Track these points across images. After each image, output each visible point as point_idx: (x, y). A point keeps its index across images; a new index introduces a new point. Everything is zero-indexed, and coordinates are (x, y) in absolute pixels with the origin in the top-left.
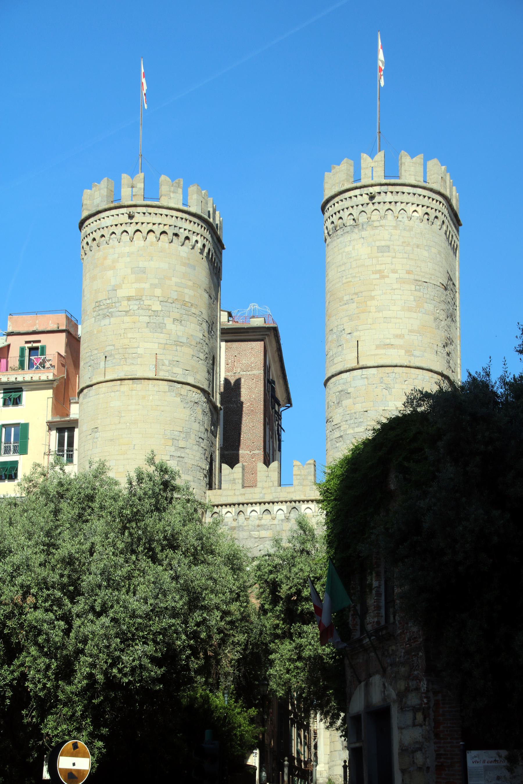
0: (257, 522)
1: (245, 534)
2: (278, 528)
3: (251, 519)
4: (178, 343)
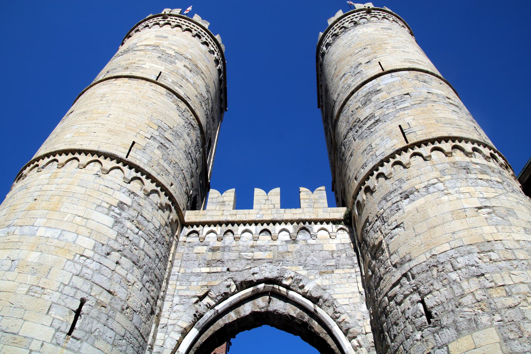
0: (251, 243)
1: (234, 255)
2: (281, 249)
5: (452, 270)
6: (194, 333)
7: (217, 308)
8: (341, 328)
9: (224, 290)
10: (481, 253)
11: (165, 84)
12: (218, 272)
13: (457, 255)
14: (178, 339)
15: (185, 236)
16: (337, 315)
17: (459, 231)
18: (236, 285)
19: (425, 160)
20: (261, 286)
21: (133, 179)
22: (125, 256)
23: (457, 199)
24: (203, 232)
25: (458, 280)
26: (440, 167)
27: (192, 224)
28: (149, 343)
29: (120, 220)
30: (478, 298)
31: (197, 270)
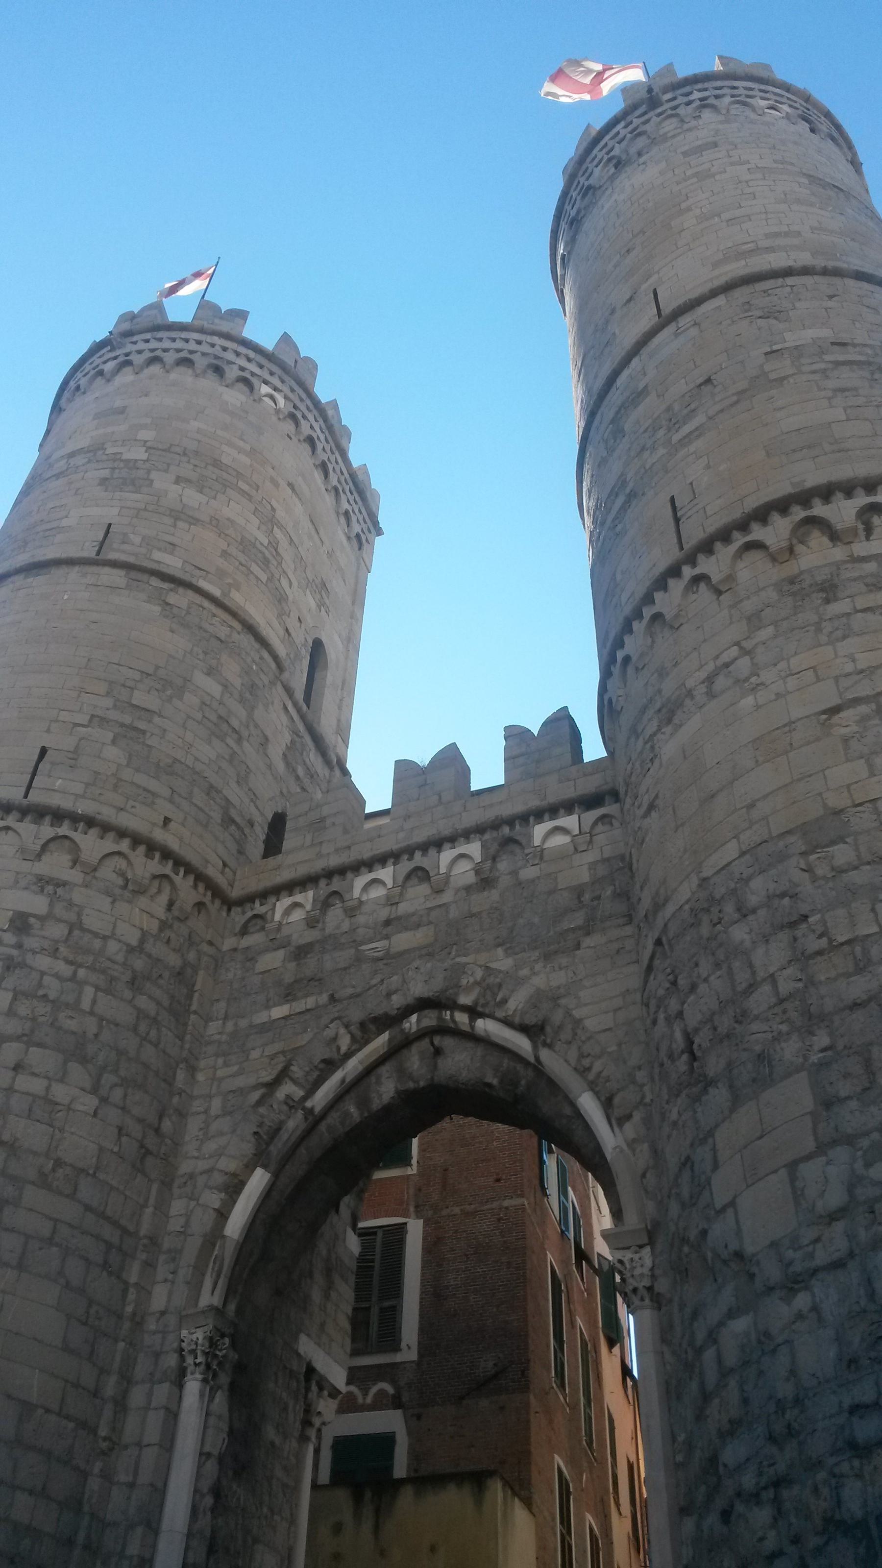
0: (384, 913)
1: (344, 957)
2: (454, 913)
3: (365, 908)
4: (180, 515)
5: (736, 916)
6: (259, 1180)
7: (308, 1104)
8: (597, 1094)
9: (320, 1053)
10: (813, 852)
11: (123, 557)
12: (308, 1010)
13: (751, 870)
14: (216, 1207)
15: (236, 935)
16: (586, 1062)
17: (766, 796)
18: (350, 1033)
19: (719, 593)
20: (412, 1023)
21: (44, 847)
22: (40, 1045)
23: (778, 696)
24: (273, 914)
25: (748, 944)
26: (749, 606)
27: (250, 899)
28: (142, 1233)
29: (20, 959)
30: (785, 987)
31: (261, 1017)
